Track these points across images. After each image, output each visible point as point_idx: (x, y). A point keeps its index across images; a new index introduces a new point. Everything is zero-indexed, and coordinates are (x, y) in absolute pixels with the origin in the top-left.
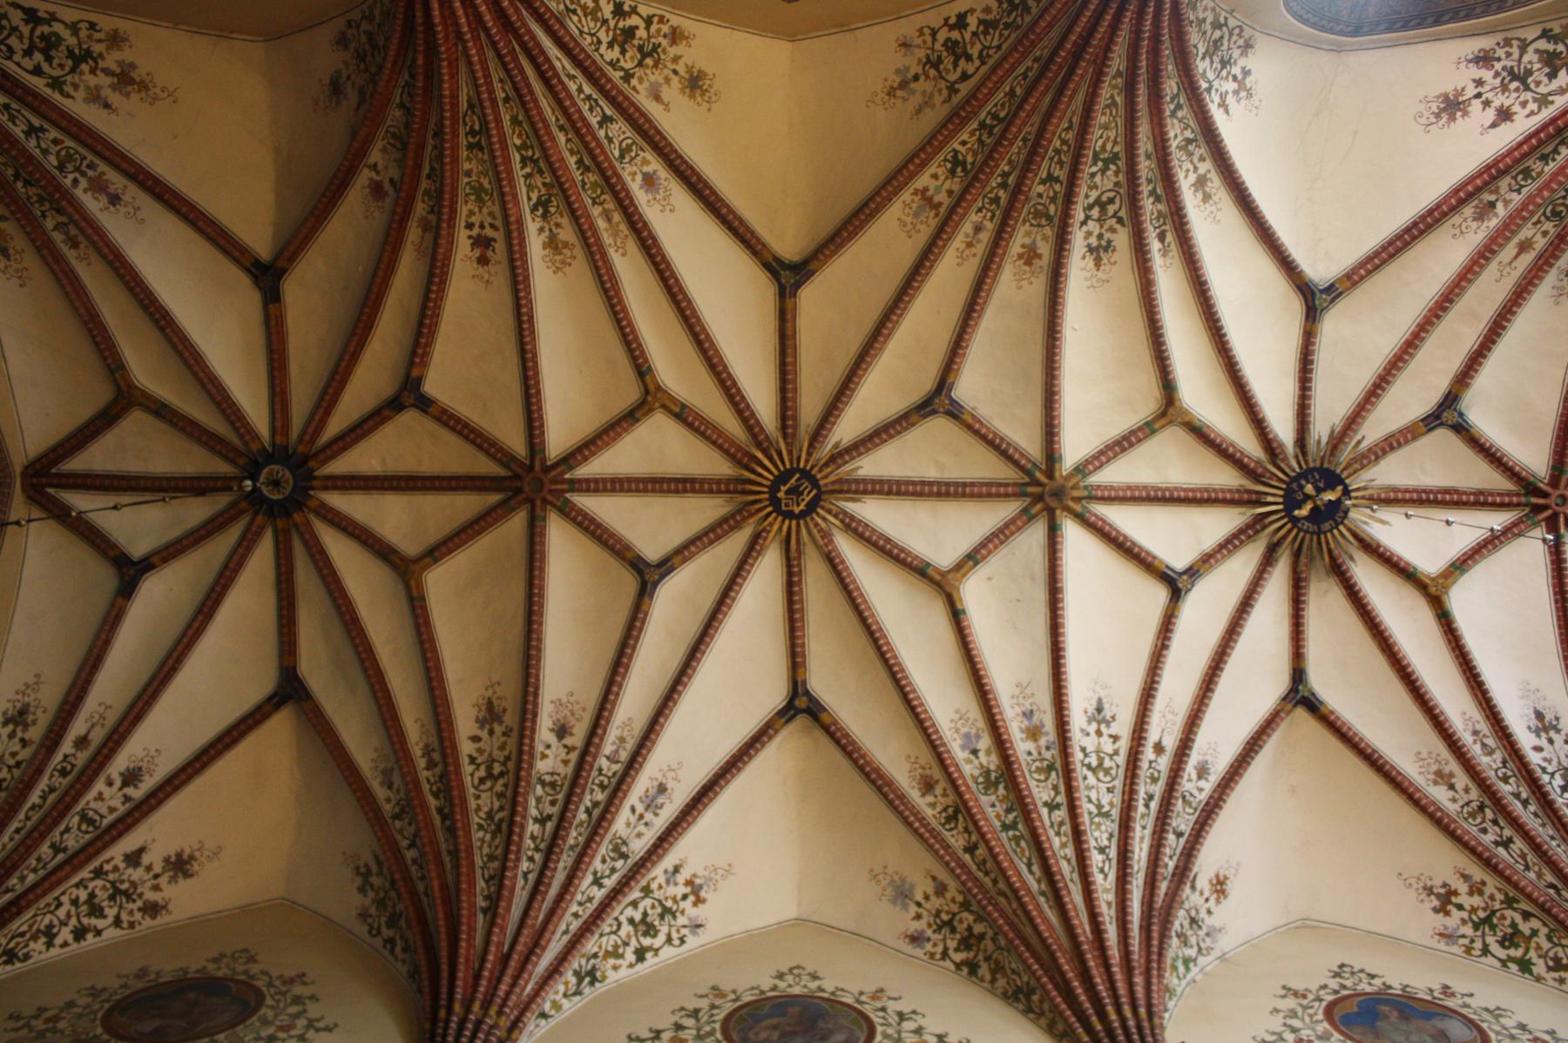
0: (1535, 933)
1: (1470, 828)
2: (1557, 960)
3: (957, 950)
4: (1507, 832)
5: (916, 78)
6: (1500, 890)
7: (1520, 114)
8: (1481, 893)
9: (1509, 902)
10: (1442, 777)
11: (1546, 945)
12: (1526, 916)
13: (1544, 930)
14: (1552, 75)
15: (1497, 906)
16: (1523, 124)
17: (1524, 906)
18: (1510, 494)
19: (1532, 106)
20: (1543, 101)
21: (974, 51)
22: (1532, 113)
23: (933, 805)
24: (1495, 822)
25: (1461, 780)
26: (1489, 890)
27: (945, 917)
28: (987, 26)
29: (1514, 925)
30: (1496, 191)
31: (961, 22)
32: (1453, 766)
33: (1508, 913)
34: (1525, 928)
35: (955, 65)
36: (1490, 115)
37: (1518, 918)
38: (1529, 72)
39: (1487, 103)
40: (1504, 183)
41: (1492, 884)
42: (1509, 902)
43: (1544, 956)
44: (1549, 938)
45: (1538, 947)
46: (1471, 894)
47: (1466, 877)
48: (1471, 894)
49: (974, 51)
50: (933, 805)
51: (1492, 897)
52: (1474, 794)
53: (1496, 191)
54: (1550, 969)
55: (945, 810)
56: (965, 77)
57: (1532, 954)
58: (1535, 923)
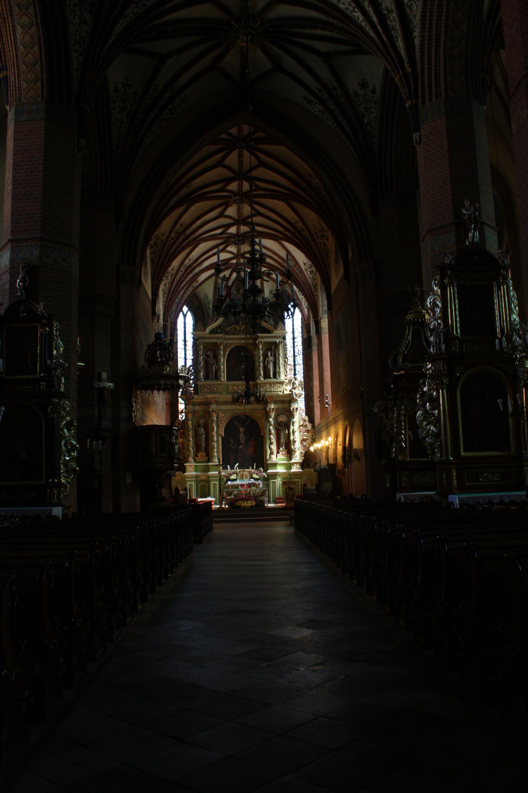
0: (169, 280)
1: (183, 266)
2: (166, 284)
3: (153, 242)
4: (183, 271)
5: (320, 225)
6: (174, 273)
7: (305, 267)
8: (172, 270)
9: (172, 275)
10: (190, 260)
11: (167, 282)
12: (171, 278)
13: (169, 281)
14: (310, 272)
15: (171, 273)
16: (303, 267)
17: (172, 277)
18: (240, 252)
19: (306, 268)
20: (306, 270)
21: (322, 241)
22: (304, 268)
23: (178, 228)
24: (184, 269)
25: (190, 263)
26: (173, 272)
27: (158, 237)
28: (325, 245)
29: (168, 276)
30: (293, 262)
31: (327, 240)
32: (192, 261)
33: (170, 275)
34: (169, 278)
35: (320, 235)
36: (305, 262)
37: (170, 277)
38: (311, 268)
39: (307, 262)
40: (294, 263)
41: (174, 272)
42: (172, 275)
43: (166, 282)
44: (169, 282)
45: (167, 281)
46: (171, 269)
47: (174, 268)
48: (171, 269)
49: (322, 241)
50: (178, 228)
51: (172, 272)
52: (188, 265)
53: (293, 262)
54: (164, 284)
55: (178, 230)
56: (318, 237)
57: (165, 281)
58: (170, 279)
